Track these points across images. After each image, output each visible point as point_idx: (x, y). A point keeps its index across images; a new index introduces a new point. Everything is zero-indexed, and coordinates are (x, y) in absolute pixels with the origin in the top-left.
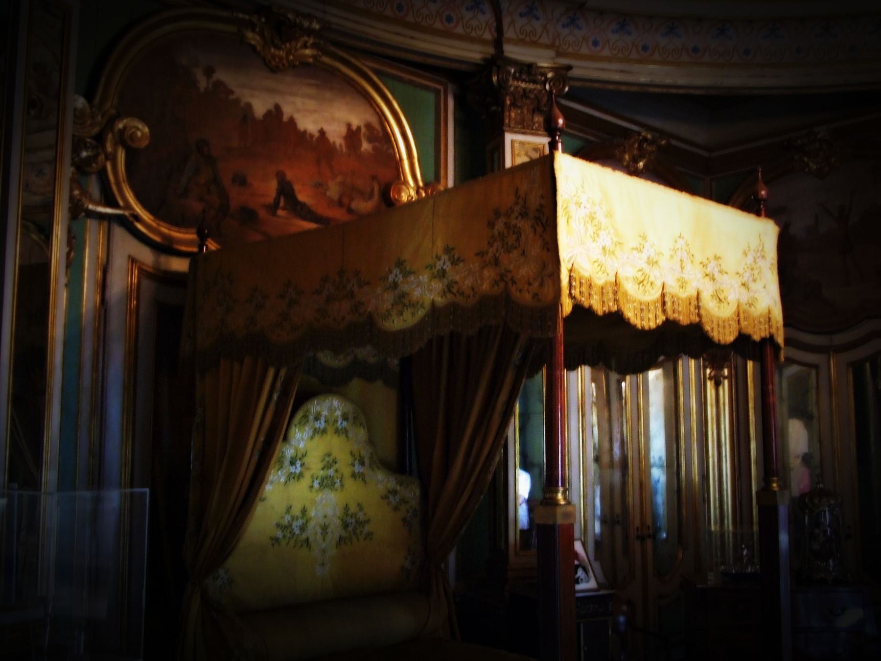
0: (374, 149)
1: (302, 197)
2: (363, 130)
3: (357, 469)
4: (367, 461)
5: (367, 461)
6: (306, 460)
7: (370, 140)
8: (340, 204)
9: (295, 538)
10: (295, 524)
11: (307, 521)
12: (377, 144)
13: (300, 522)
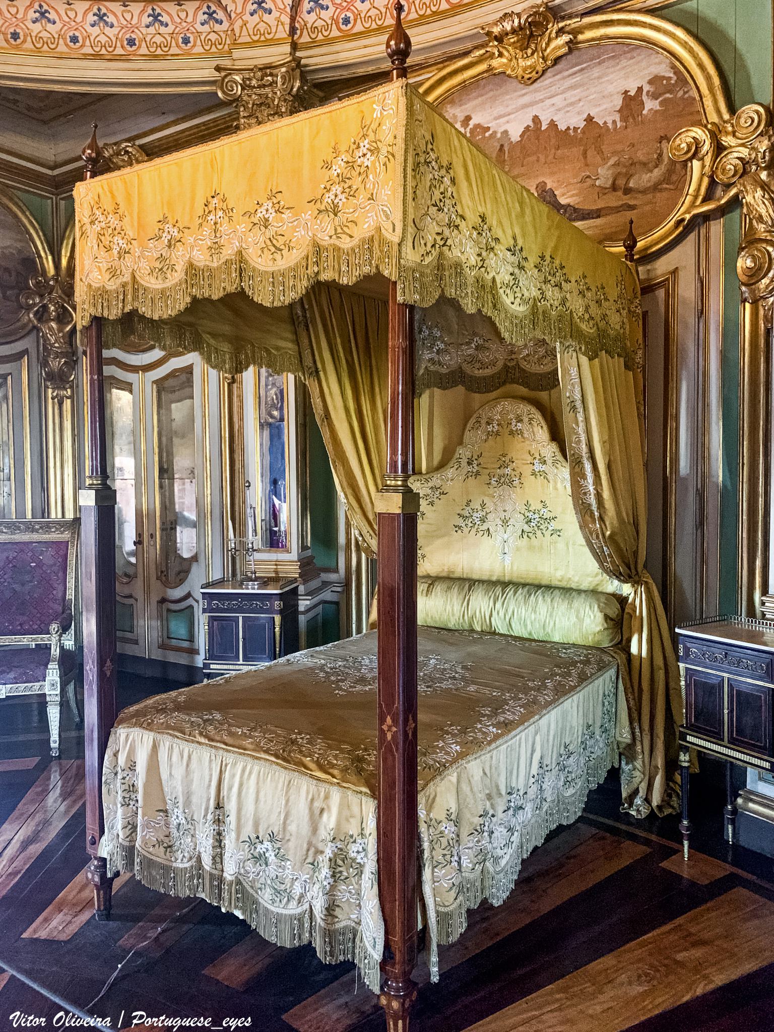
0: (661, 104)
1: (563, 201)
2: (646, 88)
3: (538, 467)
4: (549, 462)
5: (549, 462)
6: (481, 460)
7: (654, 96)
8: (614, 188)
9: (476, 526)
10: (475, 514)
11: (487, 513)
12: (668, 95)
13: (481, 514)
